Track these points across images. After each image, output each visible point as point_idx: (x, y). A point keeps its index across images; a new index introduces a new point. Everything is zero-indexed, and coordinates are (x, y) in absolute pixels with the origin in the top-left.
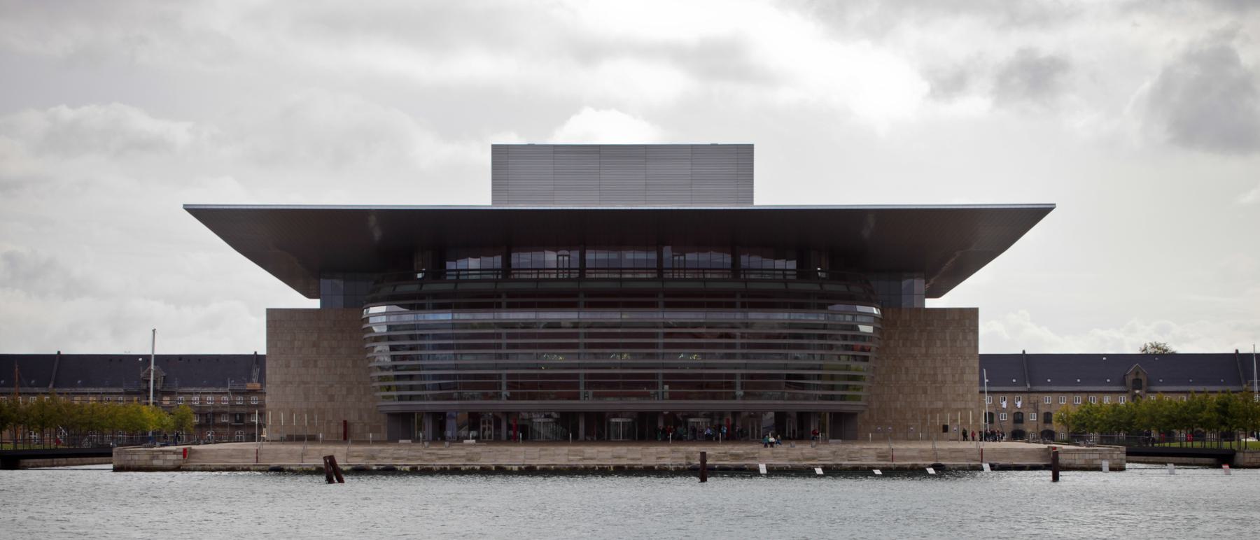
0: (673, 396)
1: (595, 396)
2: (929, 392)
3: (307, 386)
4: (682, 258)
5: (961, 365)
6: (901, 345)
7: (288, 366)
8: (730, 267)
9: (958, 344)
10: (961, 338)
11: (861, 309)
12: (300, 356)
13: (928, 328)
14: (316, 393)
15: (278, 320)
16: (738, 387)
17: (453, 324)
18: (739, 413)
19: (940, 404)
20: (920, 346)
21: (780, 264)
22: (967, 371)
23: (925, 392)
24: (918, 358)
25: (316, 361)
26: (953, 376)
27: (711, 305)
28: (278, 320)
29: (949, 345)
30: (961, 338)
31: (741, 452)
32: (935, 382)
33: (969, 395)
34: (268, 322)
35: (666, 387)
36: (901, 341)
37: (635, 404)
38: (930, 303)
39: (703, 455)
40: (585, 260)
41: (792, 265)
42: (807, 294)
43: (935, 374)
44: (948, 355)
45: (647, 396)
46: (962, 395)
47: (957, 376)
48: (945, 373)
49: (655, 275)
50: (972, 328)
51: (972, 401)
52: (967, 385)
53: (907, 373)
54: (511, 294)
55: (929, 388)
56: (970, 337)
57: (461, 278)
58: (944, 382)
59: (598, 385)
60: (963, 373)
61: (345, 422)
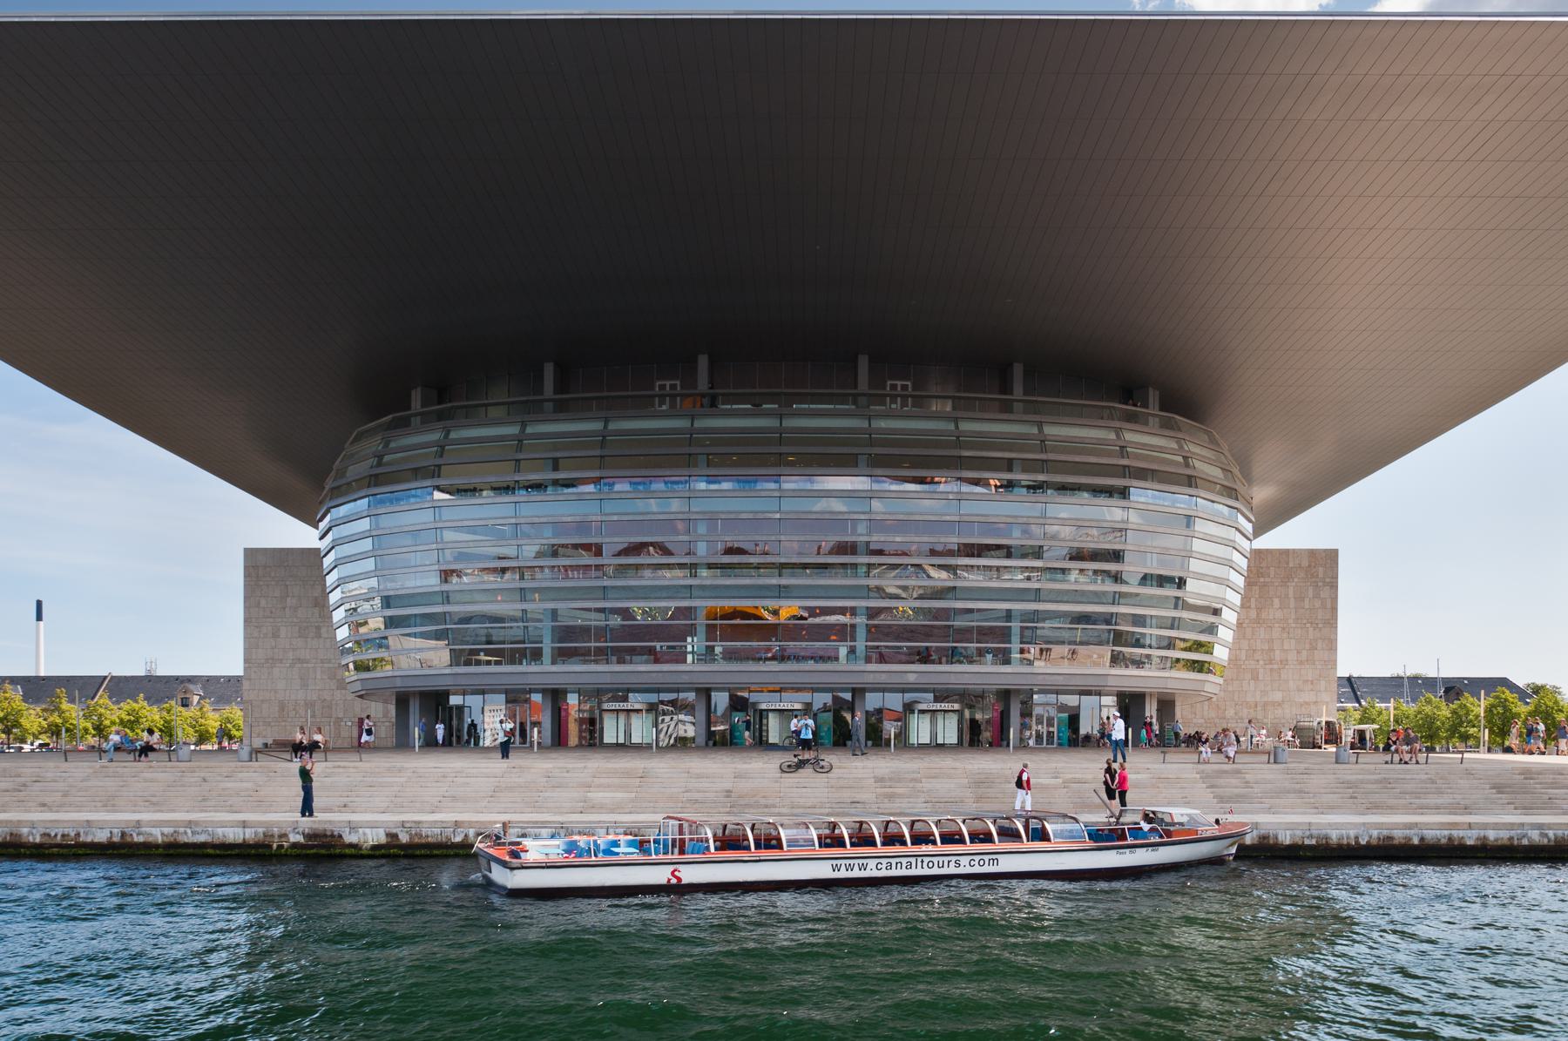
2: (1260, 678)
3: (305, 665)
7: (275, 635)
9: (1307, 604)
12: (295, 620)
14: (318, 677)
18: (1018, 691)
20: (1249, 607)
23: (1255, 678)
24: (1244, 625)
25: (318, 628)
29: (1292, 604)
30: (1311, 595)
32: (1271, 661)
44: (1291, 621)
47: (1304, 653)
48: (1285, 648)
50: (1328, 580)
51: (1326, 690)
52: (1319, 667)
55: (1261, 671)
56: (1325, 593)
58: (1284, 662)
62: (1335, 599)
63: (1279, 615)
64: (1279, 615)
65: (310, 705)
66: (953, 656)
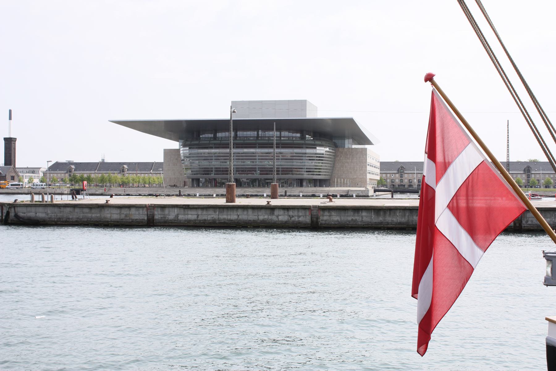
0: (260, 174)
1: (238, 174)
4: (264, 133)
5: (362, 165)
6: (344, 159)
7: (169, 165)
8: (279, 136)
9: (361, 158)
10: (362, 156)
11: (317, 148)
13: (352, 154)
15: (168, 153)
16: (280, 171)
17: (198, 153)
19: (355, 177)
21: (294, 135)
22: (364, 167)
23: (351, 173)
25: (177, 164)
26: (359, 168)
27: (242, 147)
28: (168, 153)
30: (362, 156)
31: (261, 190)
33: (364, 174)
34: (164, 153)
35: (259, 171)
36: (344, 158)
37: (250, 176)
38: (354, 146)
39: (180, 191)
40: (259, 134)
41: (298, 135)
42: (303, 144)
43: (354, 168)
44: (358, 162)
45: (253, 174)
46: (362, 174)
47: (361, 168)
48: (357, 167)
49: (279, 139)
53: (346, 167)
54: (215, 144)
55: (352, 172)
57: (222, 139)
58: (357, 170)
59: (239, 171)
60: (362, 167)
61: (184, 181)
62: (366, 158)
63: (356, 161)
64: (356, 161)
65: (175, 178)
66: (267, 174)
